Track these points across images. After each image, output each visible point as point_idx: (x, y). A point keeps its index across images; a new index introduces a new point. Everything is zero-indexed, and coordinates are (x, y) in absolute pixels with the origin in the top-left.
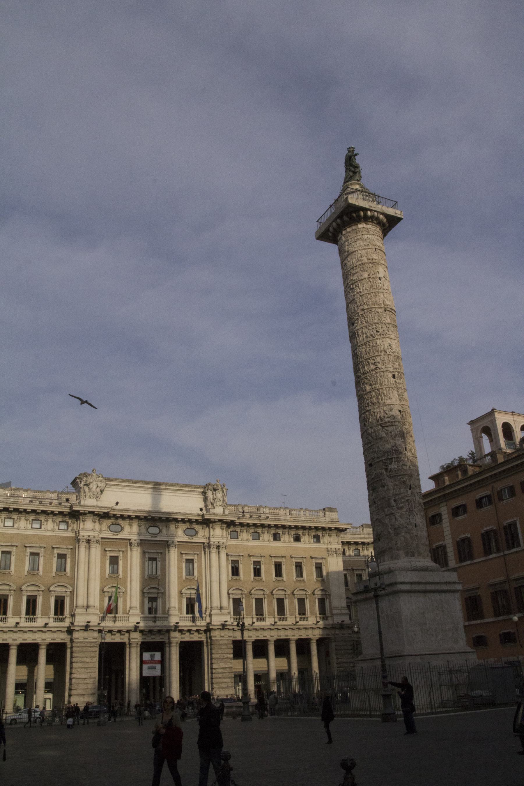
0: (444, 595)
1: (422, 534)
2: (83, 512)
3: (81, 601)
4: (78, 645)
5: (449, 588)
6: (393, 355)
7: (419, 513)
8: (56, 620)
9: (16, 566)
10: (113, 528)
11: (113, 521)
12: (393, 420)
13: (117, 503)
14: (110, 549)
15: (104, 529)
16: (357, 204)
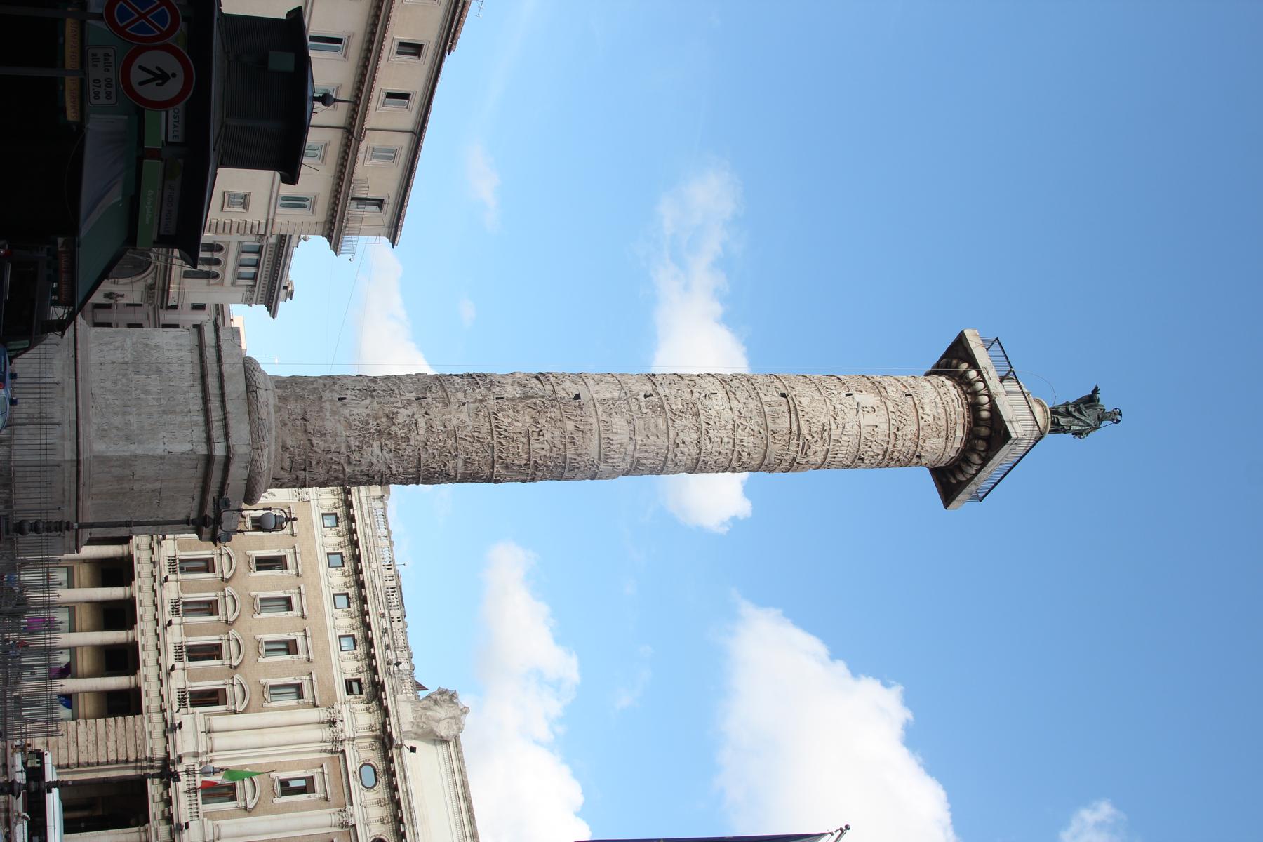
0: (201, 419)
1: (328, 413)
2: (383, 697)
3: (218, 722)
4: (139, 723)
5: (214, 426)
6: (694, 398)
7: (369, 411)
8: (182, 693)
9: (269, 619)
10: (368, 772)
11: (381, 766)
12: (552, 381)
13: (413, 750)
14: (326, 772)
15: (362, 756)
16: (972, 345)
